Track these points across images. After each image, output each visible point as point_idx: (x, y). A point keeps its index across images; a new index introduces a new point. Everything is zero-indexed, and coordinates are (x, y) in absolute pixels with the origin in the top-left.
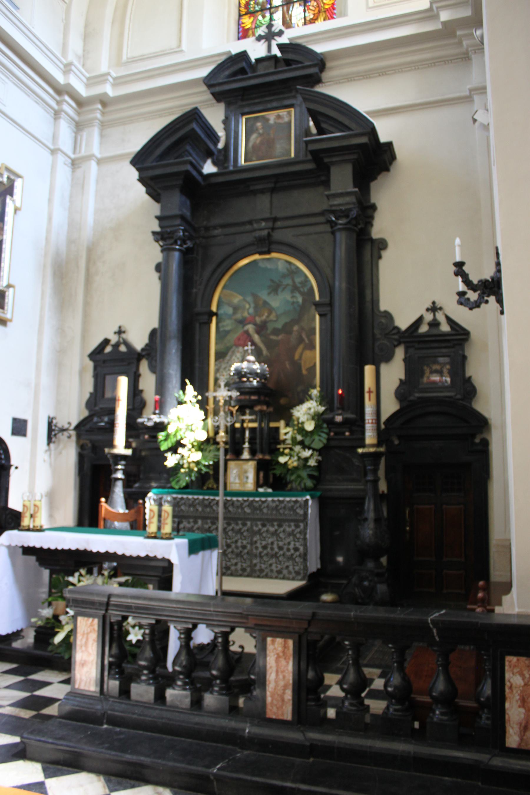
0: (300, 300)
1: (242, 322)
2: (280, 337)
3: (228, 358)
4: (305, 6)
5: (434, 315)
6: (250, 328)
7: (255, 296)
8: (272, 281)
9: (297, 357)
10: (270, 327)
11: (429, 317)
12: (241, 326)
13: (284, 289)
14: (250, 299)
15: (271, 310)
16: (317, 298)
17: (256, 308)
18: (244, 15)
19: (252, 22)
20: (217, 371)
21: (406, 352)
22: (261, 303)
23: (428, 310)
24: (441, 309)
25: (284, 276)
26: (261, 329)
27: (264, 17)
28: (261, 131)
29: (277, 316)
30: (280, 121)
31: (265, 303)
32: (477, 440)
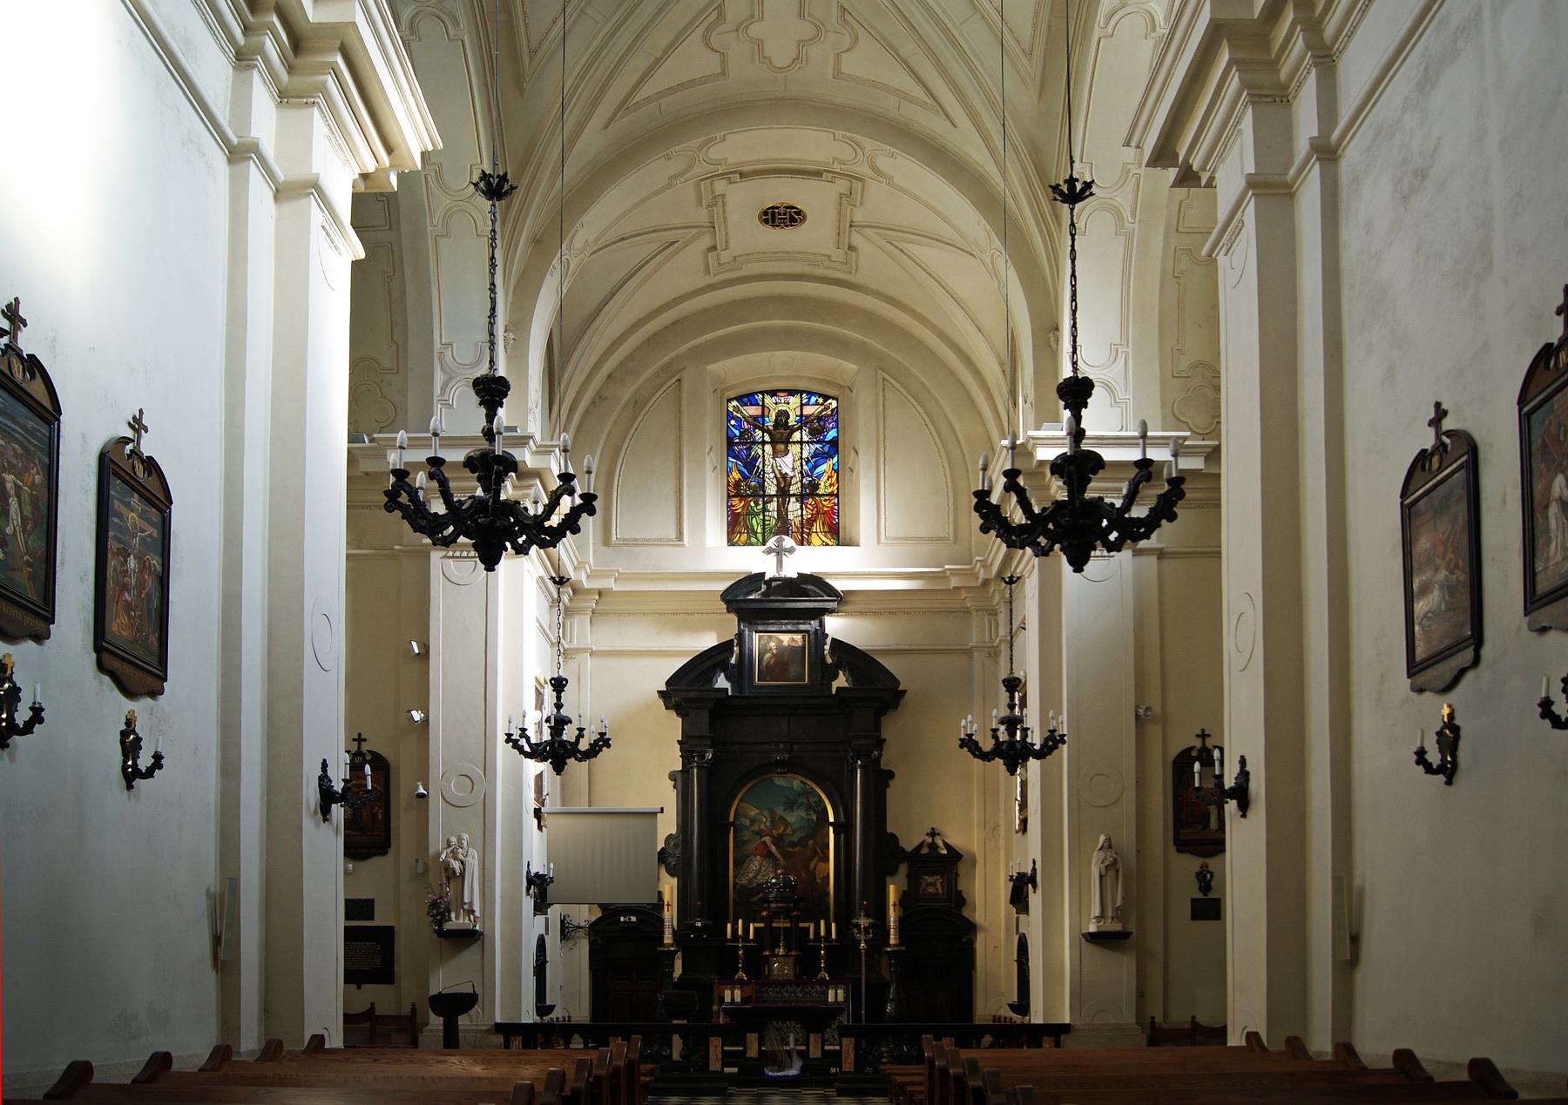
0: (814, 818)
1: (760, 834)
2: (796, 850)
3: (746, 865)
4: (802, 503)
5: (933, 840)
6: (767, 839)
7: (772, 812)
8: (787, 798)
9: (812, 867)
10: (787, 839)
11: (929, 840)
12: (758, 838)
13: (799, 807)
14: (766, 813)
15: (787, 825)
16: (831, 819)
17: (772, 822)
18: (733, 496)
19: (744, 506)
20: (735, 877)
21: (909, 870)
22: (777, 817)
23: (927, 834)
24: (938, 834)
25: (799, 795)
26: (778, 841)
27: (757, 504)
28: (774, 652)
29: (793, 831)
30: (793, 644)
31: (782, 818)
32: (964, 940)
